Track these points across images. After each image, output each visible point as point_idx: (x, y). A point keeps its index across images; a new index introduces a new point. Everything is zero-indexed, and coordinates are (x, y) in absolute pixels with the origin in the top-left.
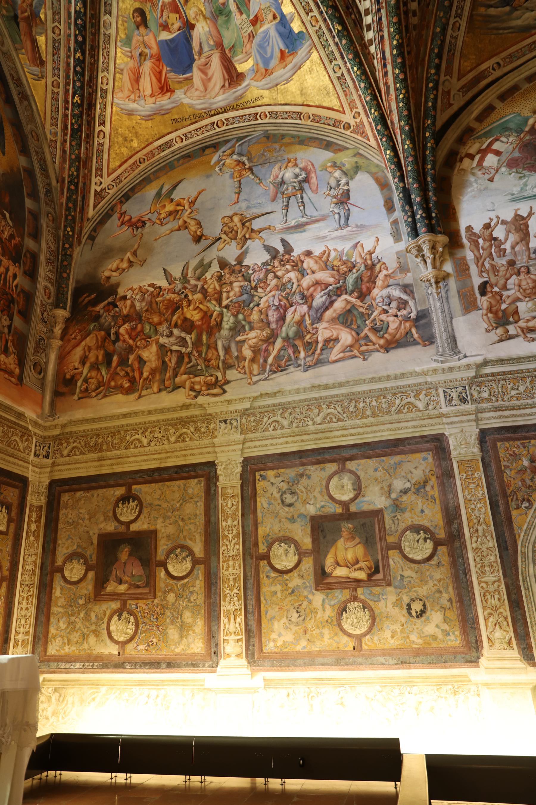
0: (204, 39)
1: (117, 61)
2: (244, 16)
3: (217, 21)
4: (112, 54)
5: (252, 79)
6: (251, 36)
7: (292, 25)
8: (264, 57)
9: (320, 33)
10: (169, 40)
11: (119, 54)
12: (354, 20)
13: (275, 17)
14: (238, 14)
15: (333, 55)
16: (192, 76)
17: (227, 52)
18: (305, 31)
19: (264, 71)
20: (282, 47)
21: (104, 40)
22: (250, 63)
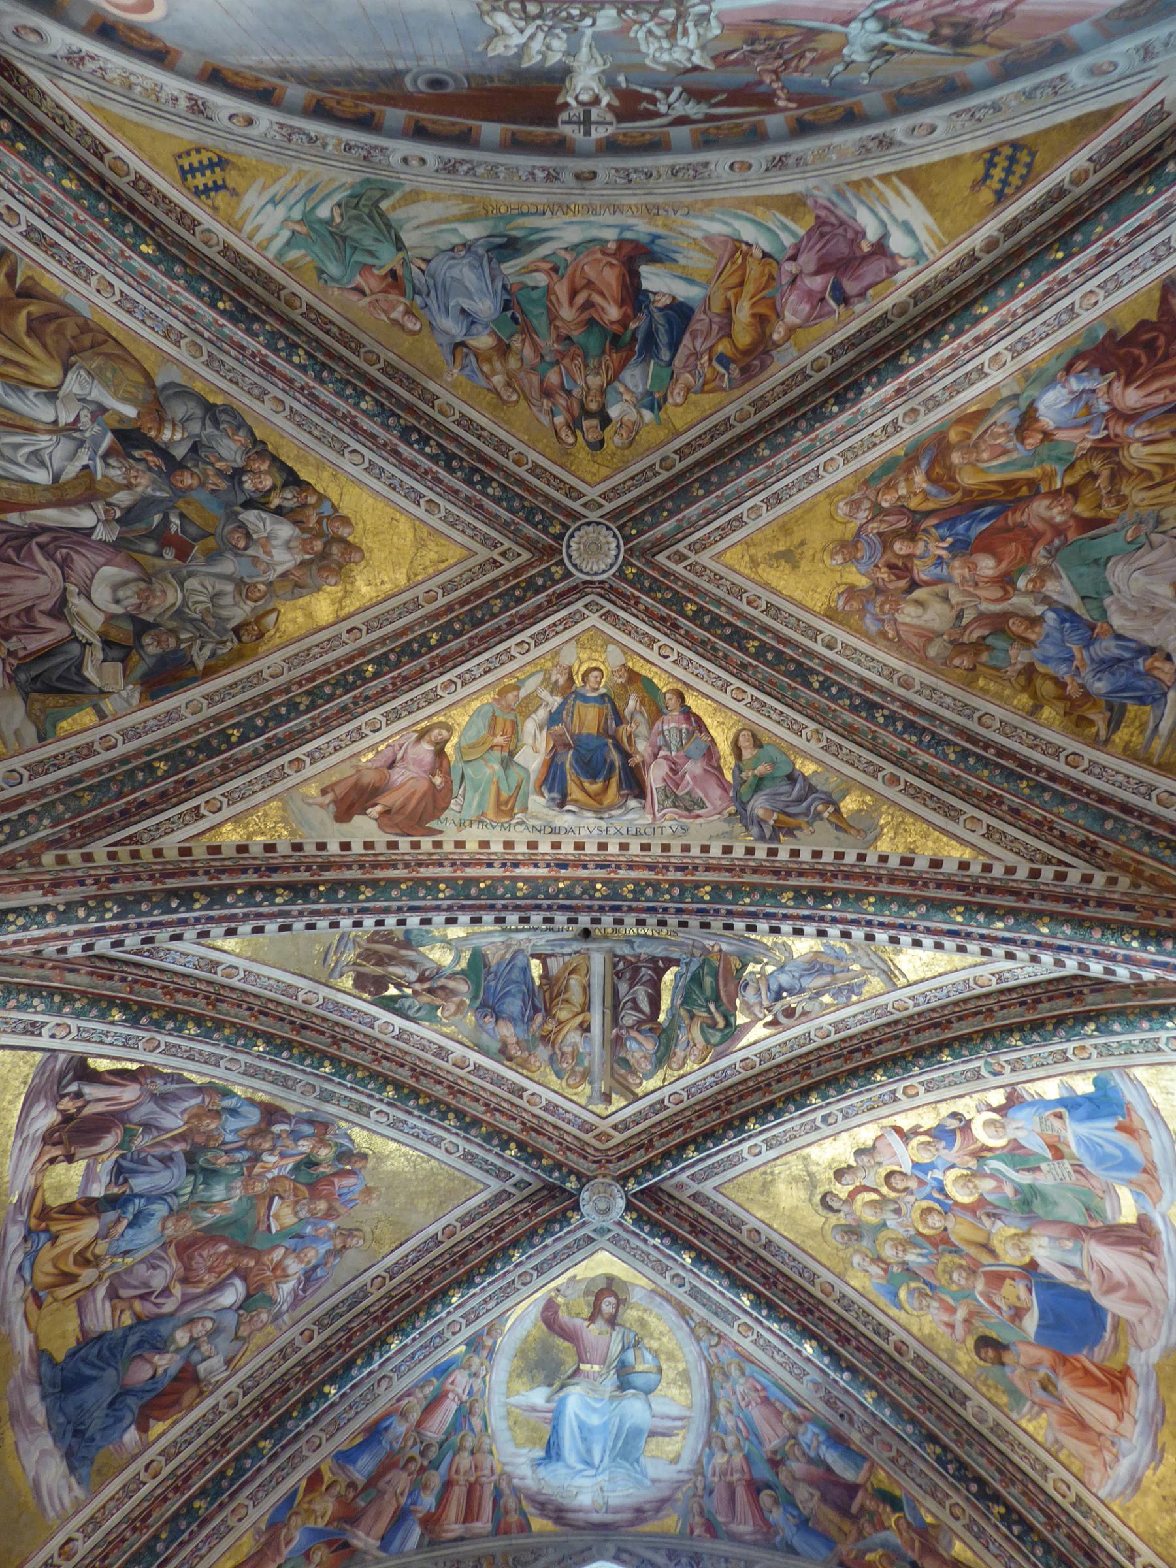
0: (1058, 1255)
1: (1040, 1439)
2: (1044, 1166)
3: (1038, 1217)
4: (1025, 1439)
5: (1155, 1205)
6: (1079, 1169)
7: (1079, 1093)
8: (1120, 1164)
9: (1104, 1051)
10: (1041, 1318)
11: (1030, 1428)
12: (1093, 991)
13: (1060, 1116)
14: (1038, 1175)
15: (1148, 1041)
16: (1114, 1315)
17: (1093, 1225)
18: (1095, 1075)
19: (1144, 1176)
20: (1111, 1124)
21: (999, 1437)
22: (1125, 1194)
